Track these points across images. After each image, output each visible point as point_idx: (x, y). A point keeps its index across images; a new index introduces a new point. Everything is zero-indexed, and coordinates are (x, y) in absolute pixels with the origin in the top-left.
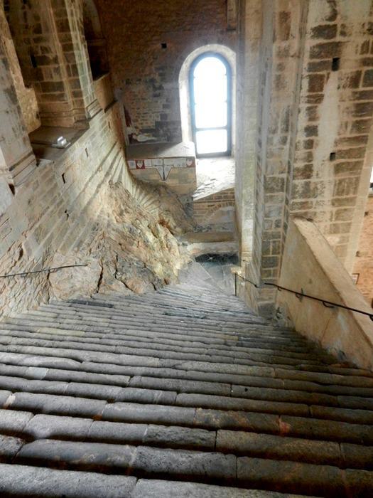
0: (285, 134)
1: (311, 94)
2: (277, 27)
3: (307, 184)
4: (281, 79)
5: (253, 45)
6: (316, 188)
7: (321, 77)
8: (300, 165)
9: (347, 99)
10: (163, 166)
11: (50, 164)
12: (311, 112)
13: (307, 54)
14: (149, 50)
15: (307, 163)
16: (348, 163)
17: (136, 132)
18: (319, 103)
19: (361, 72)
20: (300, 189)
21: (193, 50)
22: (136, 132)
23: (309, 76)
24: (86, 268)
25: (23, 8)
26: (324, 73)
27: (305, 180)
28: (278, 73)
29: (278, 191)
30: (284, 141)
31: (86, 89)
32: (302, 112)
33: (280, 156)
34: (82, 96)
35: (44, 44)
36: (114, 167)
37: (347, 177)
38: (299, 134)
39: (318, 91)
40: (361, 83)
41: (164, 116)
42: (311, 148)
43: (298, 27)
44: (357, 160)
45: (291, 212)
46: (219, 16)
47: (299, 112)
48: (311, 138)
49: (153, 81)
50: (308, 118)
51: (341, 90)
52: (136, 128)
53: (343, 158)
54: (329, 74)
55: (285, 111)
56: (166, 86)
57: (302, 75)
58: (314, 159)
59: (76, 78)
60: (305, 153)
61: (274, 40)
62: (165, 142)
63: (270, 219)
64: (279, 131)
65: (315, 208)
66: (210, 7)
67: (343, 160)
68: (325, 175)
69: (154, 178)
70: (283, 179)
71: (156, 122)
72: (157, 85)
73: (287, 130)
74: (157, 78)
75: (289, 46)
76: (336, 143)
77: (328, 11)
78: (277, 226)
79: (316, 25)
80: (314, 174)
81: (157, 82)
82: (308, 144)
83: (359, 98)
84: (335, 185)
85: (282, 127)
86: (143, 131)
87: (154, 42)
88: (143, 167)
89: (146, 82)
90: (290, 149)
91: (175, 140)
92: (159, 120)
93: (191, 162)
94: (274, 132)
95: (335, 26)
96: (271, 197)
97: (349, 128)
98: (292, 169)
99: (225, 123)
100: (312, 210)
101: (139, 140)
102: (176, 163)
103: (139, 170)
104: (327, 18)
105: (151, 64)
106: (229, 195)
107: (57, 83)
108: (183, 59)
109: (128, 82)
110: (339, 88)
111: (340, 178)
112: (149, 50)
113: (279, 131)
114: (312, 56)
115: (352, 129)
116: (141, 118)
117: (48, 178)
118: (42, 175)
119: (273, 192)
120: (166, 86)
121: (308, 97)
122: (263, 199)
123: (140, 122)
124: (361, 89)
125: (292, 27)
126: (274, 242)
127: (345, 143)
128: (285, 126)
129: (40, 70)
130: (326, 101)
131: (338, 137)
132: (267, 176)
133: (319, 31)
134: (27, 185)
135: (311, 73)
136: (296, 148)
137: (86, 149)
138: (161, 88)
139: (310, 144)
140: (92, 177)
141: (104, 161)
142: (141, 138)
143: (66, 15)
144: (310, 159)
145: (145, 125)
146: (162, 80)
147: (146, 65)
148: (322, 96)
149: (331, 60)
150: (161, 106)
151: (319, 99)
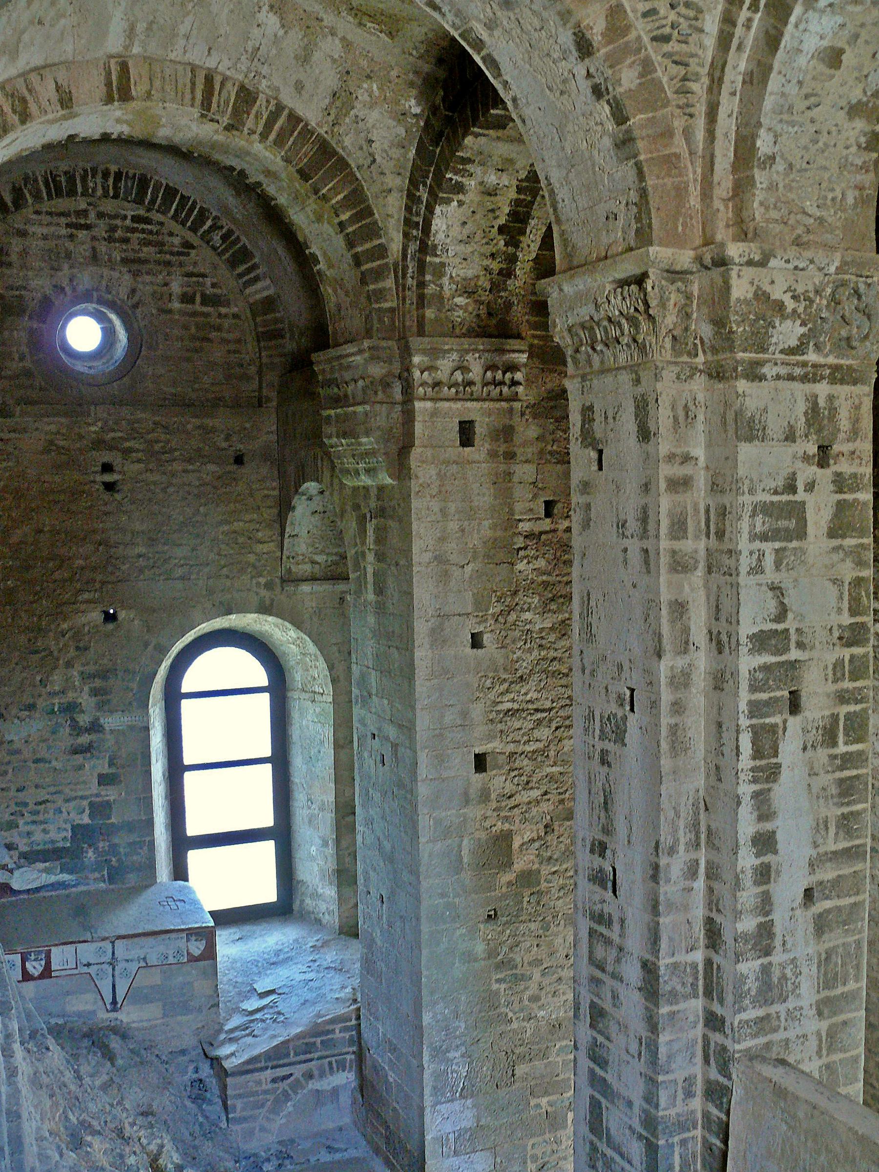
1: (758, 763)
4: (679, 733)
5: (433, 631)
6: (784, 977)
7: (773, 728)
8: (748, 924)
9: (822, 772)
12: (762, 802)
13: (744, 685)
14: (65, 626)
15: (761, 919)
16: (839, 909)
18: (775, 781)
19: (838, 715)
20: (752, 985)
23: (751, 726)
26: (777, 719)
27: (760, 962)
28: (673, 721)
29: (686, 997)
30: (692, 872)
33: (686, 908)
37: (840, 941)
38: (742, 852)
40: (841, 739)
42: (768, 882)
43: (705, 631)
44: (852, 900)
45: (737, 1047)
46: (259, 548)
47: (739, 803)
48: (766, 859)
49: (71, 708)
50: (756, 814)
53: (827, 898)
54: (785, 722)
55: (691, 801)
56: (111, 722)
58: (775, 906)
60: (756, 896)
63: (670, 1077)
65: (785, 1029)
67: (828, 904)
69: (82, 1007)
70: (694, 966)
74: (86, 700)
76: (812, 866)
77: (772, 606)
79: (755, 630)
80: (778, 942)
81: (83, 712)
82: (762, 874)
83: (842, 768)
84: (819, 967)
86: (30, 857)
87: (83, 607)
88: (47, 973)
89: (53, 712)
90: (710, 890)
92: (86, 820)
93: (202, 945)
94: (672, 851)
95: (787, 630)
96: (672, 1015)
97: (832, 830)
98: (727, 936)
99: (266, 818)
100: (780, 1035)
101: (16, 886)
102: (154, 951)
103: (31, 985)
104: (772, 617)
105: (69, 665)
106: (338, 1035)
108: (163, 651)
110: (805, 749)
111: (827, 946)
112: (65, 626)
113: (682, 848)
114: (753, 689)
115: (837, 834)
119: (677, 1003)
120: (111, 722)
121: (752, 770)
123: (23, 828)
124: (842, 748)
125: (693, 627)
127: (828, 864)
130: (785, 775)
131: (814, 853)
133: (761, 641)
135: (754, 721)
136: (738, 885)
138: (95, 727)
139: (764, 874)
144: (767, 908)
145: (38, 836)
146: (100, 706)
147: (56, 667)
148: (778, 766)
149: (786, 693)
151: (772, 773)
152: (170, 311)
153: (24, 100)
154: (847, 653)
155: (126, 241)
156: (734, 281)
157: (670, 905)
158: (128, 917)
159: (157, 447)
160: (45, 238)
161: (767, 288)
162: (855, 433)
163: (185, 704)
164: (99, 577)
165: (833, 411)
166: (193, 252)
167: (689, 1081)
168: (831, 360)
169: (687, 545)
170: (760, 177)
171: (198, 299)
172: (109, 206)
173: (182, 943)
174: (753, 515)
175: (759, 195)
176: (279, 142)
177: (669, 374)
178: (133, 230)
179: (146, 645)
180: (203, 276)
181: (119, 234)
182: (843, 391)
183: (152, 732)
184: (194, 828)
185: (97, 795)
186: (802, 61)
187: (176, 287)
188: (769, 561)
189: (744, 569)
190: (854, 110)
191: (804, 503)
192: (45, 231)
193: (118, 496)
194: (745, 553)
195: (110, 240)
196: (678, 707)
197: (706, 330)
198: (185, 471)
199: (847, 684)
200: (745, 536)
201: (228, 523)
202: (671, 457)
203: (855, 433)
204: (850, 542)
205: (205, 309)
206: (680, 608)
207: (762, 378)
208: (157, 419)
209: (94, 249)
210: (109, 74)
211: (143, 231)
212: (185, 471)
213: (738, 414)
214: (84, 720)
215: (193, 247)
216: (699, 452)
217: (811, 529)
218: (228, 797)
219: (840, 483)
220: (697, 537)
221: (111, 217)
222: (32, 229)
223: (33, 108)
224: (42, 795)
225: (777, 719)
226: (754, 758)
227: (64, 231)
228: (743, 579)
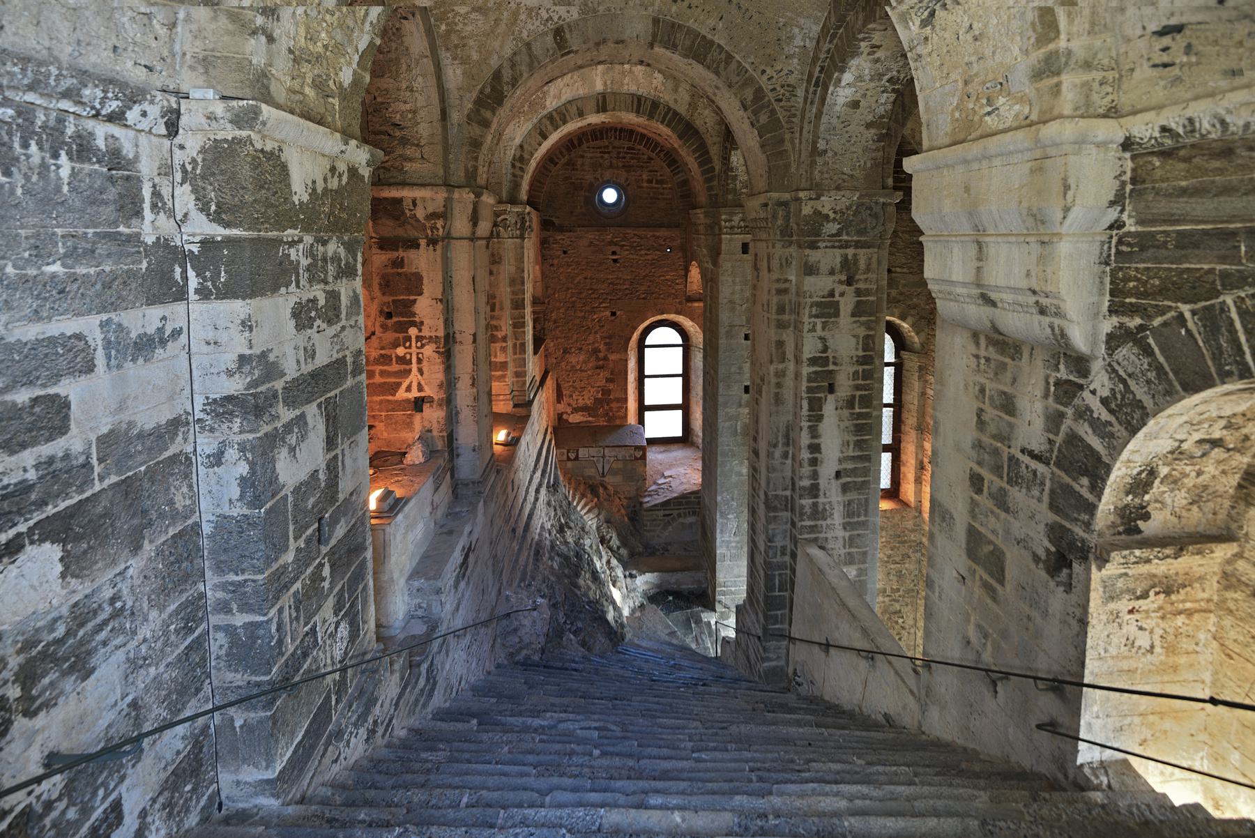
2: (774, 352)
3: (815, 505)
8: (806, 483)
13: (805, 379)
24: (535, 613)
26: (822, 395)
48: (817, 455)
51: (839, 411)
61: (771, 362)
68: (833, 495)
70: (786, 497)
73: (788, 444)
77: (820, 346)
78: (783, 554)
94: (775, 446)
96: (775, 517)
97: (851, 446)
114: (809, 381)
122: (763, 519)
124: (857, 410)
126: (780, 575)
132: (771, 493)
133: (813, 361)
136: (801, 466)
139: (814, 462)
151: (820, 418)
154: (860, 368)
156: (803, 207)
157: (774, 470)
161: (820, 209)
162: (868, 270)
165: (856, 261)
167: (784, 548)
168: (855, 238)
169: (786, 317)
170: (819, 160)
174: (811, 306)
175: (819, 168)
177: (779, 245)
182: (861, 252)
186: (838, 108)
188: (819, 327)
189: (806, 330)
190: (869, 126)
191: (838, 302)
196: (779, 385)
197: (795, 227)
199: (860, 382)
202: (778, 280)
203: (868, 270)
204: (863, 319)
206: (780, 344)
207: (818, 248)
213: (806, 263)
216: (793, 278)
217: (842, 313)
219: (858, 292)
220: (790, 314)
225: (822, 395)
228: (805, 334)
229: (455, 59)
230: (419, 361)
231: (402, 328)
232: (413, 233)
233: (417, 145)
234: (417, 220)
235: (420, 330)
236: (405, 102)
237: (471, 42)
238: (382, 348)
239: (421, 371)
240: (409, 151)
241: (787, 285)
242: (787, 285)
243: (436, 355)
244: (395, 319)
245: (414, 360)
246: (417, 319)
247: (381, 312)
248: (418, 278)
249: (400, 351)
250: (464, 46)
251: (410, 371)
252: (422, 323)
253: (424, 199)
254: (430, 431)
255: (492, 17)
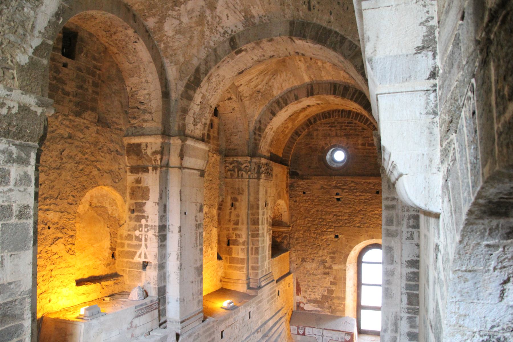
0: (395, 335)
1: (410, 306)
4: (389, 291)
10: (323, 336)
11: (213, 322)
14: (323, 238)
17: (304, 301)
21: (361, 242)
22: (304, 301)
23: (408, 293)
25: (231, 209)
31: (263, 266)
32: (403, 319)
34: (258, 270)
35: (238, 232)
36: (273, 330)
39: (416, 305)
41: (330, 291)
47: (401, 319)
49: (324, 262)
50: (409, 325)
52: (305, 297)
55: (394, 315)
56: (335, 267)
57: (401, 292)
59: (257, 256)
62: (329, 314)
64: (389, 331)
66: (376, 212)
71: (323, 296)
72: (327, 265)
74: (328, 259)
75: (394, 269)
79: (409, 259)
81: (326, 262)
85: (392, 327)
86: (310, 301)
88: (304, 334)
91: (338, 314)
92: (326, 294)
101: (305, 309)
102: (336, 336)
105: (324, 249)
107: (241, 259)
108: (351, 248)
109: (303, 260)
112: (323, 238)
113: (389, 331)
116: (310, 290)
117: (208, 333)
118: (204, 329)
120: (335, 267)
121: (408, 308)
125: (395, 256)
128: (394, 327)
129: (231, 248)
134: (190, 336)
135: (408, 291)
137: (249, 313)
138: (330, 268)
140: (249, 337)
141: (266, 323)
142: (308, 307)
143: (259, 215)
145: (312, 296)
150: (329, 283)
152: (358, 149)
153: (286, 100)
155: (345, 129)
158: (331, 325)
159: (352, 188)
160: (323, 130)
163: (363, 265)
164: (334, 225)
166: (365, 131)
171: (367, 144)
172: (340, 120)
173: (343, 335)
176: (355, 101)
178: (348, 126)
179: (347, 245)
180: (368, 138)
181: (343, 128)
183: (347, 272)
184: (363, 303)
185: (330, 287)
187: (360, 142)
192: (323, 129)
193: (340, 202)
194: (405, 232)
195: (341, 129)
198: (360, 195)
200: (405, 226)
201: (373, 211)
202: (387, 199)
205: (369, 147)
208: (353, 180)
209: (336, 133)
210: (308, 90)
211: (350, 126)
212: (360, 195)
214: (327, 265)
215: (365, 129)
218: (373, 296)
221: (341, 123)
222: (319, 129)
223: (289, 102)
224: (314, 284)
226: (408, 304)
227: (328, 128)
229: (171, 63)
230: (146, 240)
231: (138, 219)
232: (146, 163)
233: (150, 113)
234: (148, 156)
235: (147, 221)
236: (145, 89)
237: (179, 52)
238: (129, 231)
239: (146, 246)
240: (147, 117)
241: (394, 203)
242: (394, 203)
243: (154, 237)
244: (136, 214)
245: (143, 239)
246: (146, 214)
247: (130, 209)
248: (147, 189)
249: (137, 233)
250: (175, 54)
251: (140, 246)
252: (148, 217)
253: (151, 143)
254: (149, 283)
255: (188, 36)
